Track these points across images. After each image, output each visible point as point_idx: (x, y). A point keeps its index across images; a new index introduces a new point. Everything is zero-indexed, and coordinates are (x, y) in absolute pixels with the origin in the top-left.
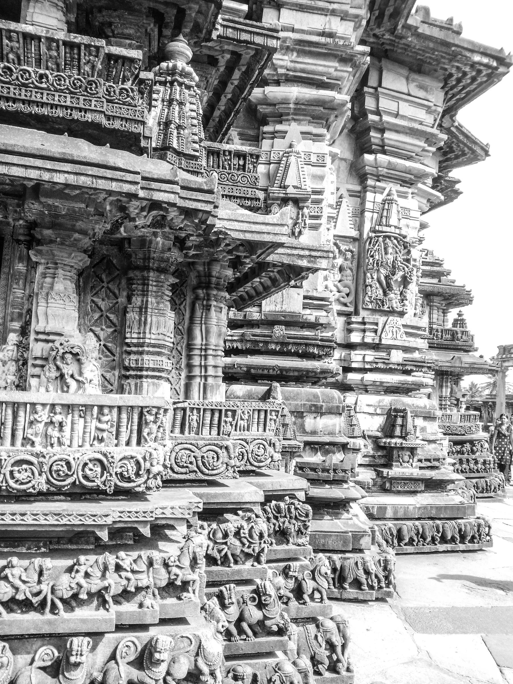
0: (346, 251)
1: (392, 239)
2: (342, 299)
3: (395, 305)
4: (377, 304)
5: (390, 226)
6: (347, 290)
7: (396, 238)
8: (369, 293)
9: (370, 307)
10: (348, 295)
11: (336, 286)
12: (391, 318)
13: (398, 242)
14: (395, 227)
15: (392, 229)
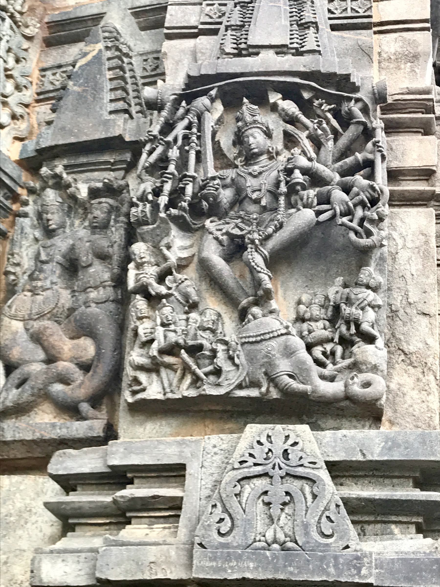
0: (94, 193)
1: (274, 97)
2: (57, 388)
3: (283, 366)
4: (186, 369)
5: (254, 50)
6: (87, 348)
7: (290, 92)
8: (144, 328)
9: (154, 390)
10: (86, 367)
11: (37, 338)
12: (253, 430)
13: (306, 107)
14: (281, 50)
15: (268, 61)
